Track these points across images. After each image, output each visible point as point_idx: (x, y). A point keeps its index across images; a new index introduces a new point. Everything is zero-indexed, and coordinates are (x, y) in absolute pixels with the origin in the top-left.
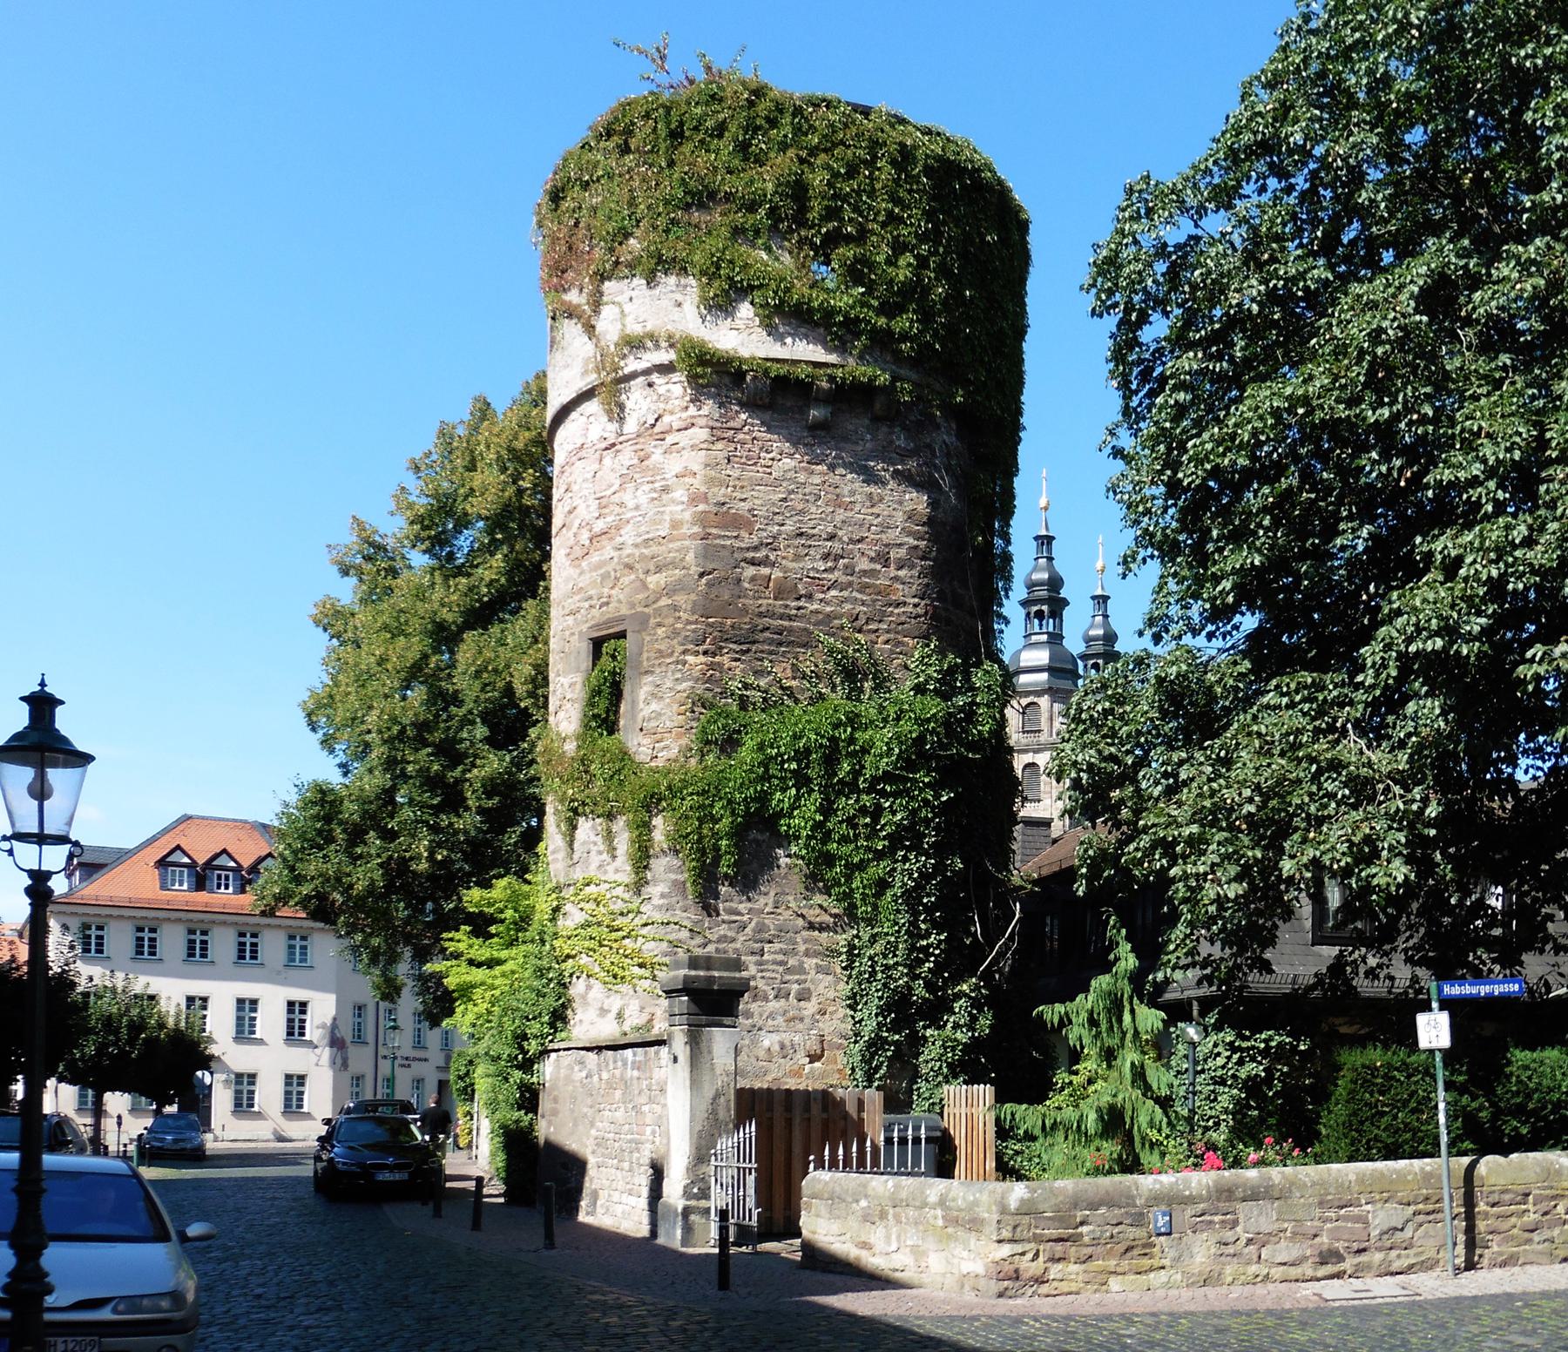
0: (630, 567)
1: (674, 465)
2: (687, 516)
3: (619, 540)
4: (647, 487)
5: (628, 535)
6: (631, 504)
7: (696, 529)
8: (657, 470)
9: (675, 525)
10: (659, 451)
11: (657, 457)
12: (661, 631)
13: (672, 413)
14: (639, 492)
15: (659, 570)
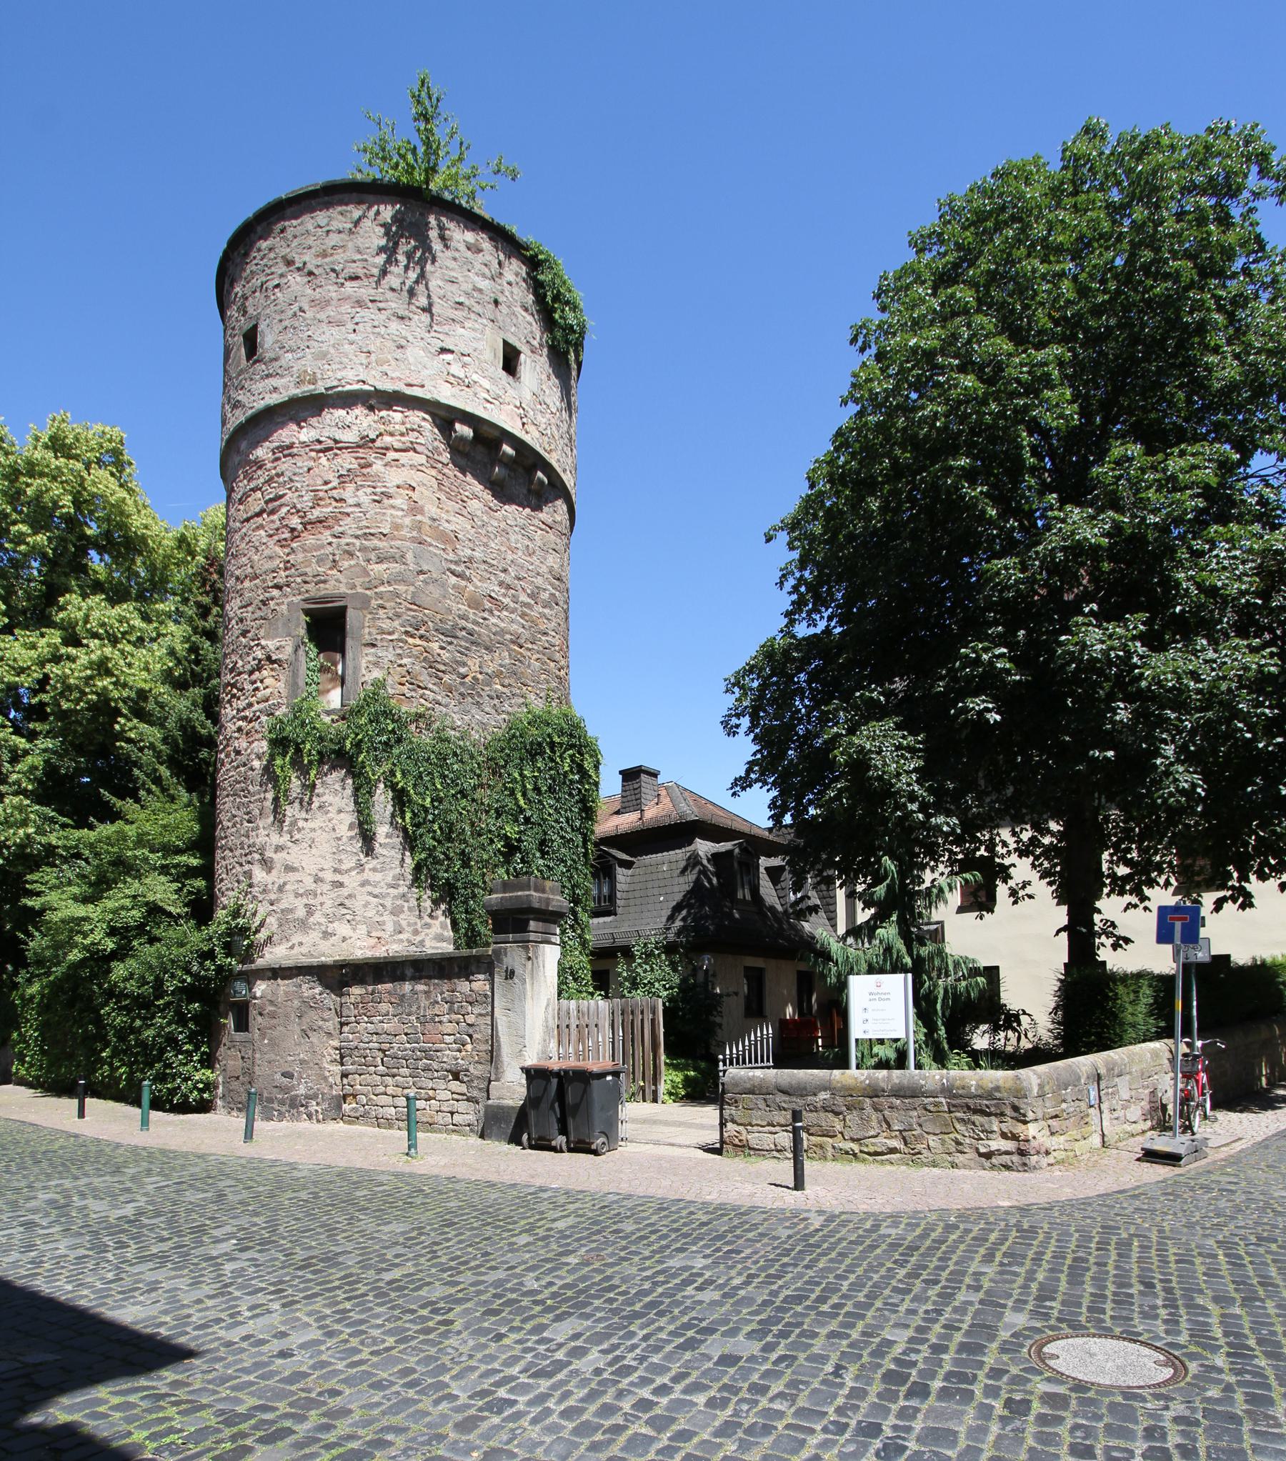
0: (351, 554)
1: (394, 478)
2: (407, 521)
3: (337, 529)
4: (369, 490)
5: (347, 525)
6: (351, 501)
7: (415, 534)
8: (377, 478)
9: (397, 527)
10: (379, 462)
11: (378, 466)
12: (381, 612)
13: (392, 434)
14: (360, 493)
15: (380, 560)
